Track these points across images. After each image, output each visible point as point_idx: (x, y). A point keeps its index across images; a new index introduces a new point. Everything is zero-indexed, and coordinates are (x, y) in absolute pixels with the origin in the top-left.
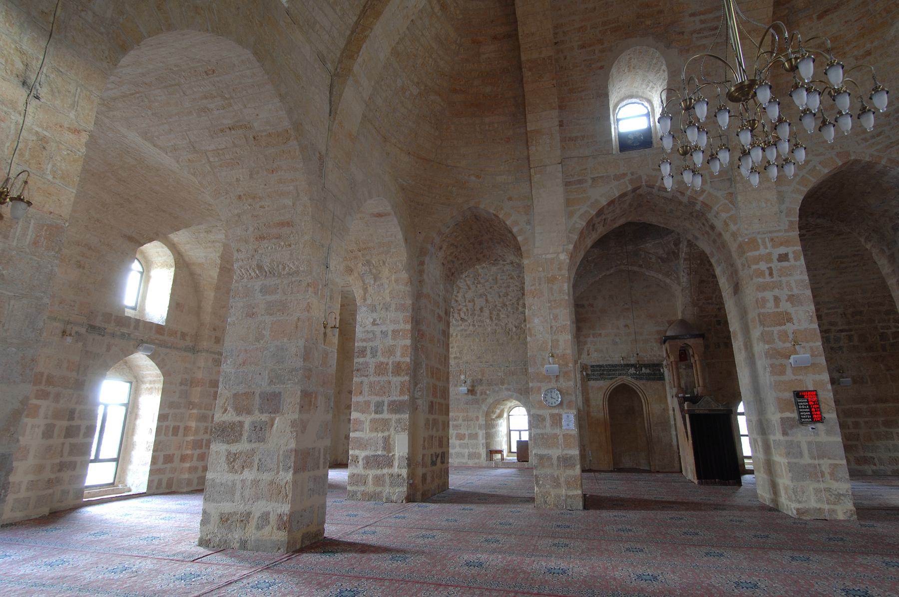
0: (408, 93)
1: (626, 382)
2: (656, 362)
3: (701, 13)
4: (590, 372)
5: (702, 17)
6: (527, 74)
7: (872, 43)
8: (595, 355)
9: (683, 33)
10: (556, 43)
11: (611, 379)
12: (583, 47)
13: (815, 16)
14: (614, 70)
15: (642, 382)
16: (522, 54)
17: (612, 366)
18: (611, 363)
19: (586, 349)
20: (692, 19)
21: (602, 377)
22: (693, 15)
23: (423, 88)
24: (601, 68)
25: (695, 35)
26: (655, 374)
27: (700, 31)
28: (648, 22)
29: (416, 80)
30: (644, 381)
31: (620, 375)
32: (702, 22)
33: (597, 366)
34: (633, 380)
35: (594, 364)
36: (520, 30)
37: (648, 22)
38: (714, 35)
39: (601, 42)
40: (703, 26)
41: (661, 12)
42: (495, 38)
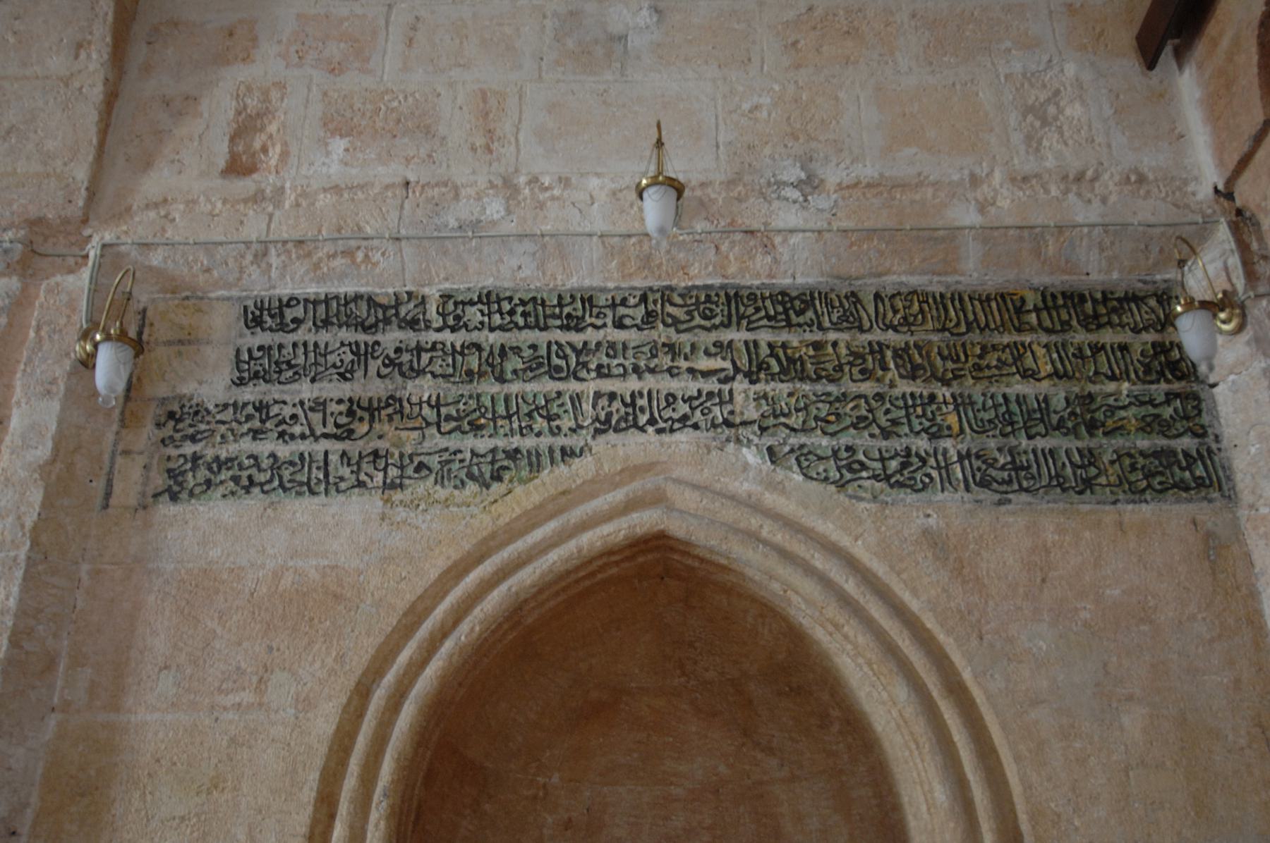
1: (689, 520)
2: (1096, 270)
4: (212, 384)
8: (317, 167)
11: (496, 470)
15: (918, 514)
17: (533, 310)
18: (517, 271)
19: (219, 108)
21: (364, 446)
26: (1088, 416)
30: (947, 509)
31: (624, 417)
33: (331, 311)
34: (796, 494)
35: (296, 282)
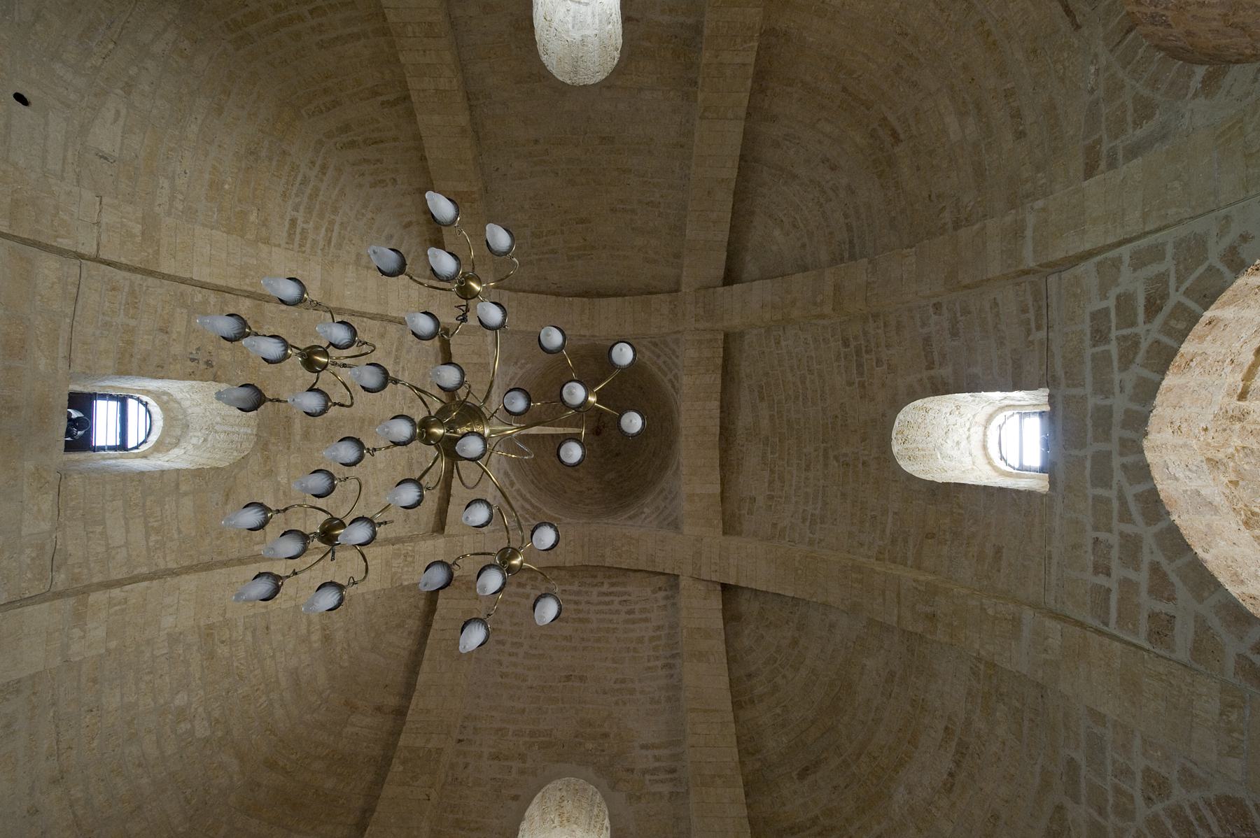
0: (184, 726)
3: (653, 746)
5: (656, 752)
6: (397, 767)
7: (879, 823)
9: (632, 770)
10: (460, 741)
12: (495, 757)
13: (794, 774)
14: (533, 811)
16: (403, 736)
20: (644, 752)
22: (644, 747)
23: (220, 734)
24: (516, 798)
25: (648, 777)
27: (654, 771)
28: (589, 746)
29: (216, 714)
32: (657, 759)
36: (414, 702)
37: (589, 746)
38: (672, 780)
39: (522, 757)
40: (657, 764)
41: (606, 735)
42: (379, 709)
